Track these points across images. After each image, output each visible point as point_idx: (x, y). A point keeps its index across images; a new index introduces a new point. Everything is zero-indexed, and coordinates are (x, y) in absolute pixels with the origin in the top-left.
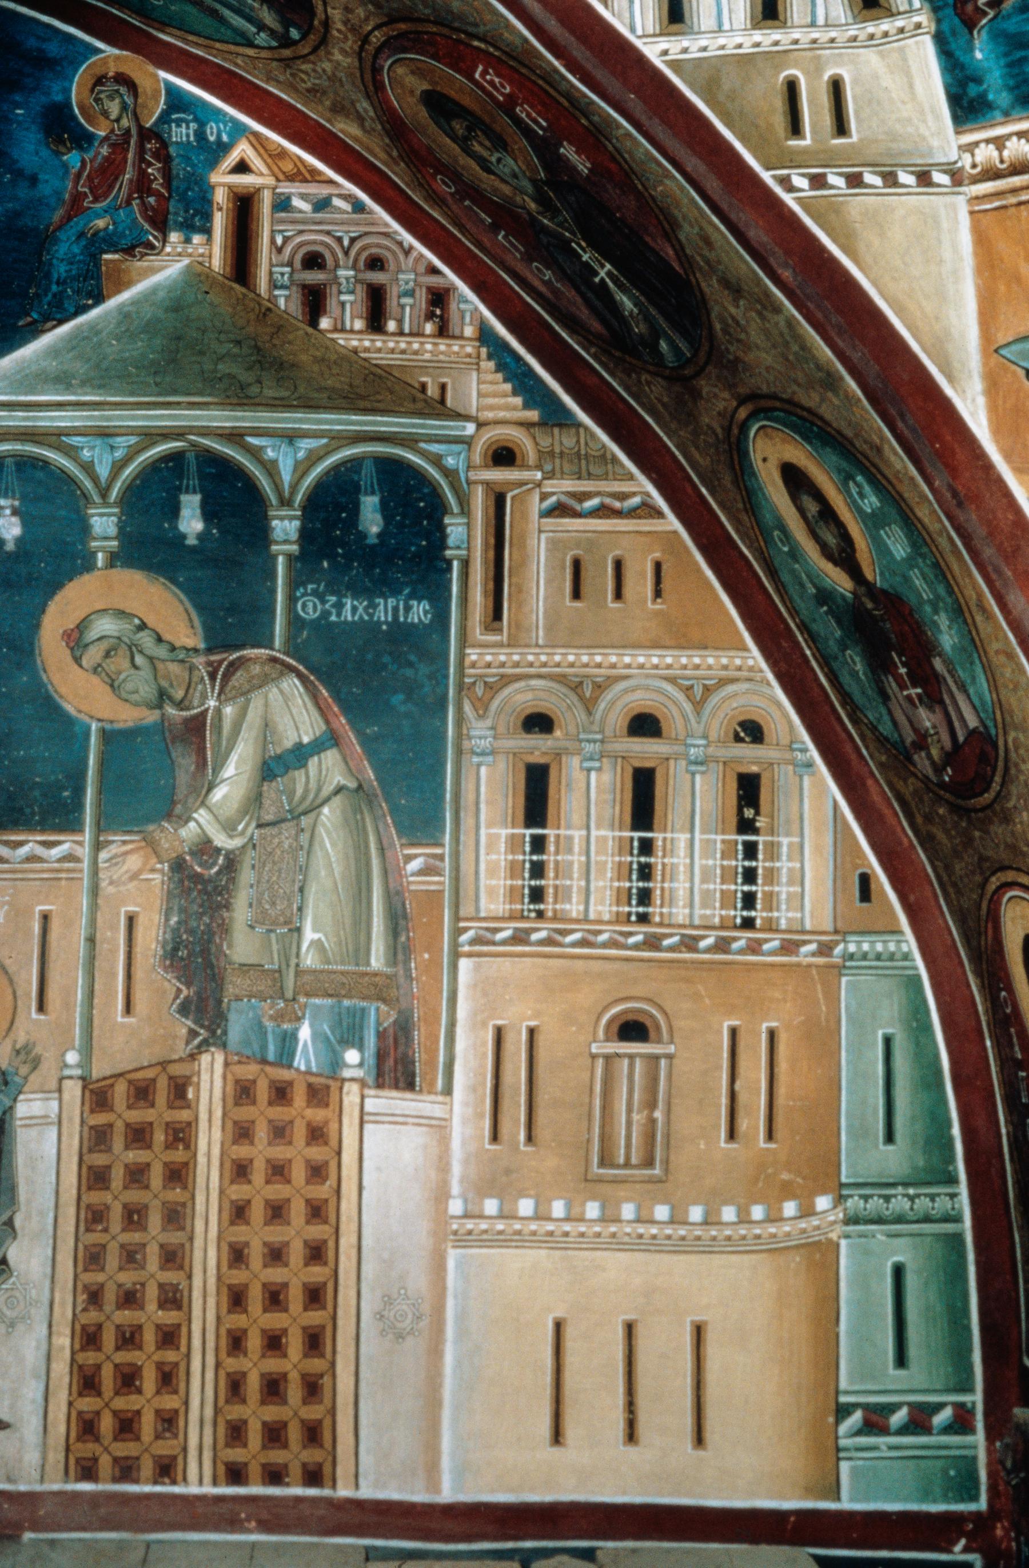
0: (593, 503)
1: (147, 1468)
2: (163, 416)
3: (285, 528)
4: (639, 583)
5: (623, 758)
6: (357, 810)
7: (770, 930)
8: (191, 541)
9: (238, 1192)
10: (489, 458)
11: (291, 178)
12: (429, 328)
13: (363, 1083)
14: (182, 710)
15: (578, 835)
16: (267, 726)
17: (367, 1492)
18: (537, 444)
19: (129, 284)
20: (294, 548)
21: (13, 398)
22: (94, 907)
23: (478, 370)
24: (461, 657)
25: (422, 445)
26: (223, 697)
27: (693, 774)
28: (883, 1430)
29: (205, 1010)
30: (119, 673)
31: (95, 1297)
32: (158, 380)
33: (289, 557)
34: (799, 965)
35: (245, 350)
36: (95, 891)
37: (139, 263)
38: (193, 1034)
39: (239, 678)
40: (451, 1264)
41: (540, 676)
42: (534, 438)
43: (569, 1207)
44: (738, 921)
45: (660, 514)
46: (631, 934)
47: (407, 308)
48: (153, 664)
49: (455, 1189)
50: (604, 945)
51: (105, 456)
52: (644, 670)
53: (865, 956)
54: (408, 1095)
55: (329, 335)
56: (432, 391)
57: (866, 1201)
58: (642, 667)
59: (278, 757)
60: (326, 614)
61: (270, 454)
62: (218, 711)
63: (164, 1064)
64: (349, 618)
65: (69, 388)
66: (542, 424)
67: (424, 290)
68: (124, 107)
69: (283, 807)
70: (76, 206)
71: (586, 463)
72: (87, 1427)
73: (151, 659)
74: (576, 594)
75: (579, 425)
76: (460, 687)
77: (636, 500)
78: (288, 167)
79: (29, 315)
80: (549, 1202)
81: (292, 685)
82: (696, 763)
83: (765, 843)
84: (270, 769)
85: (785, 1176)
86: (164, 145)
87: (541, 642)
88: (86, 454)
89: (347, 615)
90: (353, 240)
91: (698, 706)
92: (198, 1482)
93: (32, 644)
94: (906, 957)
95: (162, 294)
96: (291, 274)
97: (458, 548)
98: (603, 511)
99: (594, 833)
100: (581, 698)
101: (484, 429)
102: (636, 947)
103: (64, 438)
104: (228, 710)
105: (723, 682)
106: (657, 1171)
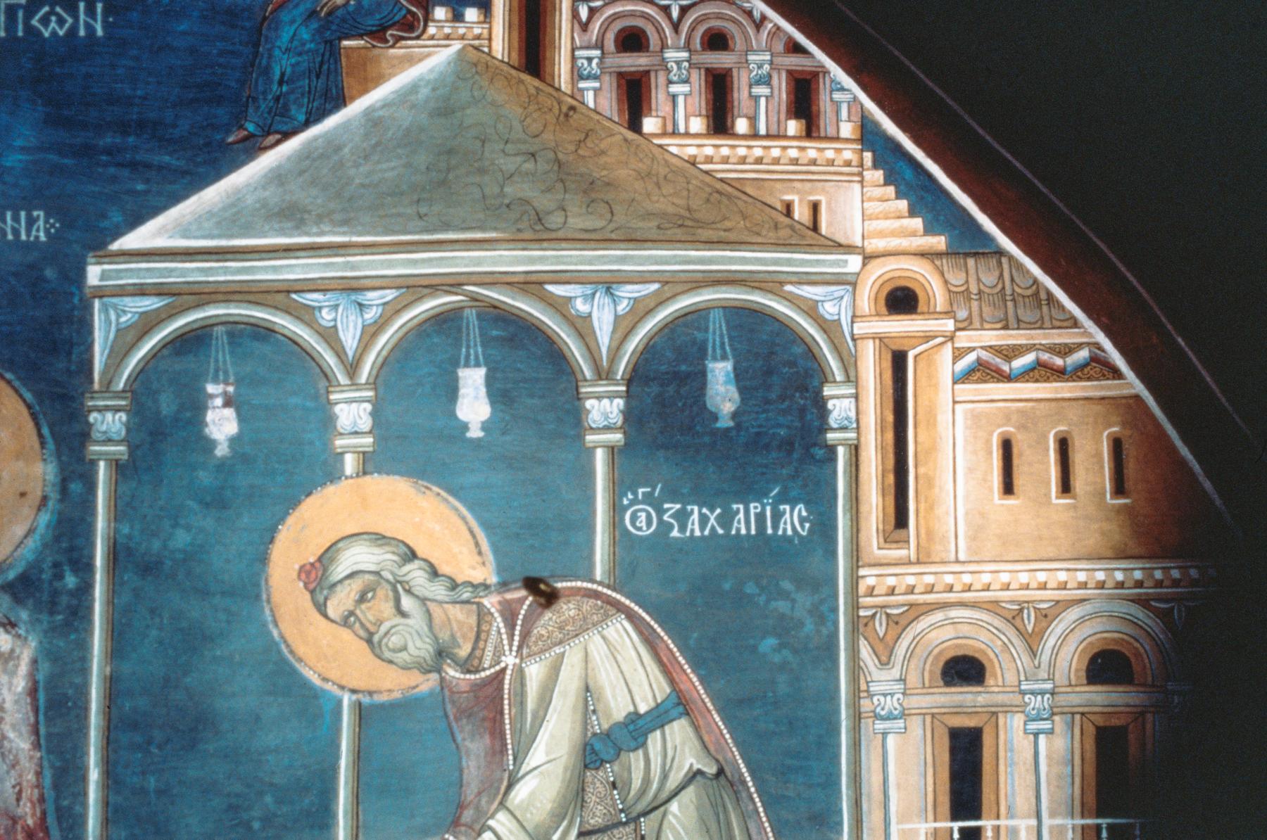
2: (430, 260)
3: (604, 409)
6: (718, 809)
10: (882, 302)
14: (469, 672)
18: (946, 282)
19: (379, 80)
20: (617, 437)
21: (224, 243)
23: (862, 182)
24: (854, 581)
25: (788, 288)
26: (525, 651)
30: (379, 623)
32: (423, 210)
33: (612, 449)
35: (542, 166)
37: (392, 51)
41: (962, 604)
42: (943, 275)
45: (1116, 374)
47: (761, 100)
48: (425, 605)
51: (352, 318)
55: (656, 141)
56: (801, 213)
59: (607, 735)
60: (665, 528)
61: (581, 306)
64: (697, 533)
65: (300, 226)
67: (784, 75)
69: (614, 805)
73: (423, 600)
74: (1008, 488)
75: (1000, 253)
76: (856, 625)
77: (1084, 354)
79: (242, 127)
81: (619, 631)
84: (593, 751)
88: (326, 316)
90: (684, 10)
93: (257, 585)
95: (424, 92)
96: (602, 58)
97: (843, 429)
99: (1047, 822)
100: (1021, 633)
101: (874, 263)
103: (294, 296)
104: (535, 672)
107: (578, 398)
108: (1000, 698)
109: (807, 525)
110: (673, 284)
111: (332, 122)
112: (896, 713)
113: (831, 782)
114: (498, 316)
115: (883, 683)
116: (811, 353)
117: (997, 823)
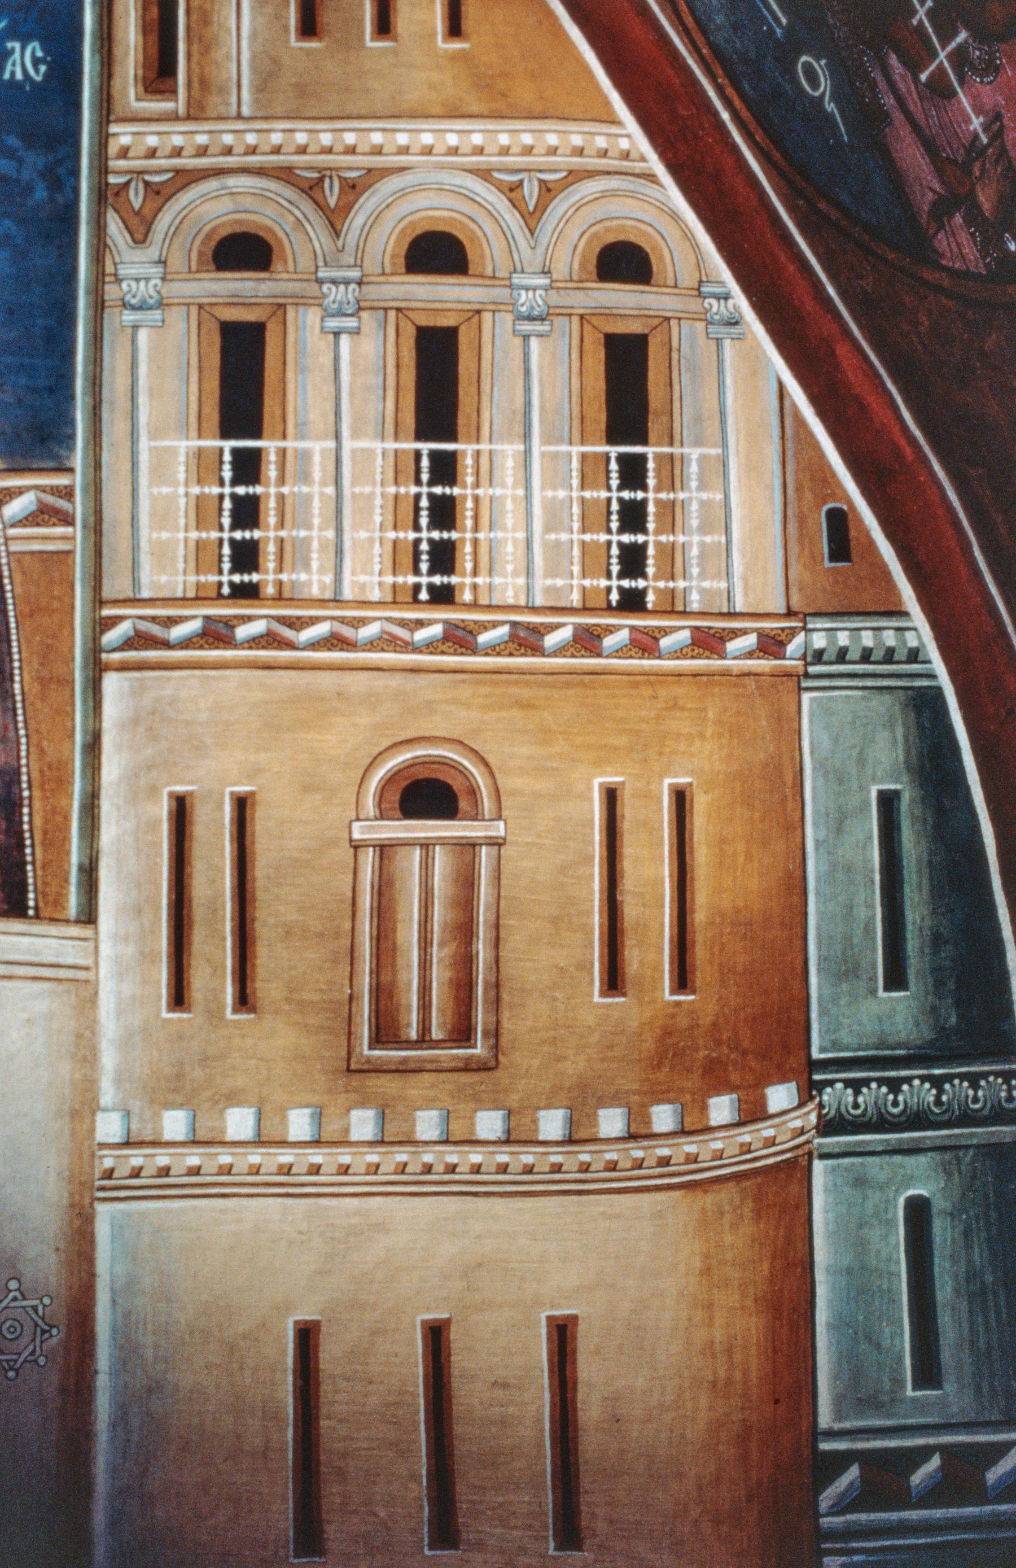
5: (399, 310)
7: (672, 612)
15: (319, 448)
27: (526, 337)
34: (726, 673)
40: (102, 1230)
43: (319, 1119)
44: (614, 597)
46: (420, 624)
49: (108, 1095)
50: (371, 645)
52: (435, 159)
54: (17, 925)
57: (857, 1093)
58: (428, 151)
76: (102, 194)
80: (282, 1112)
82: (531, 318)
83: (658, 457)
87: (246, 111)
91: (532, 219)
94: (914, 655)
99: (348, 444)
100: (321, 206)
102: (430, 647)
105: (575, 176)
106: (479, 1050)
108: (291, 287)
109: (43, 68)
112: (151, 302)
117: (281, 444)
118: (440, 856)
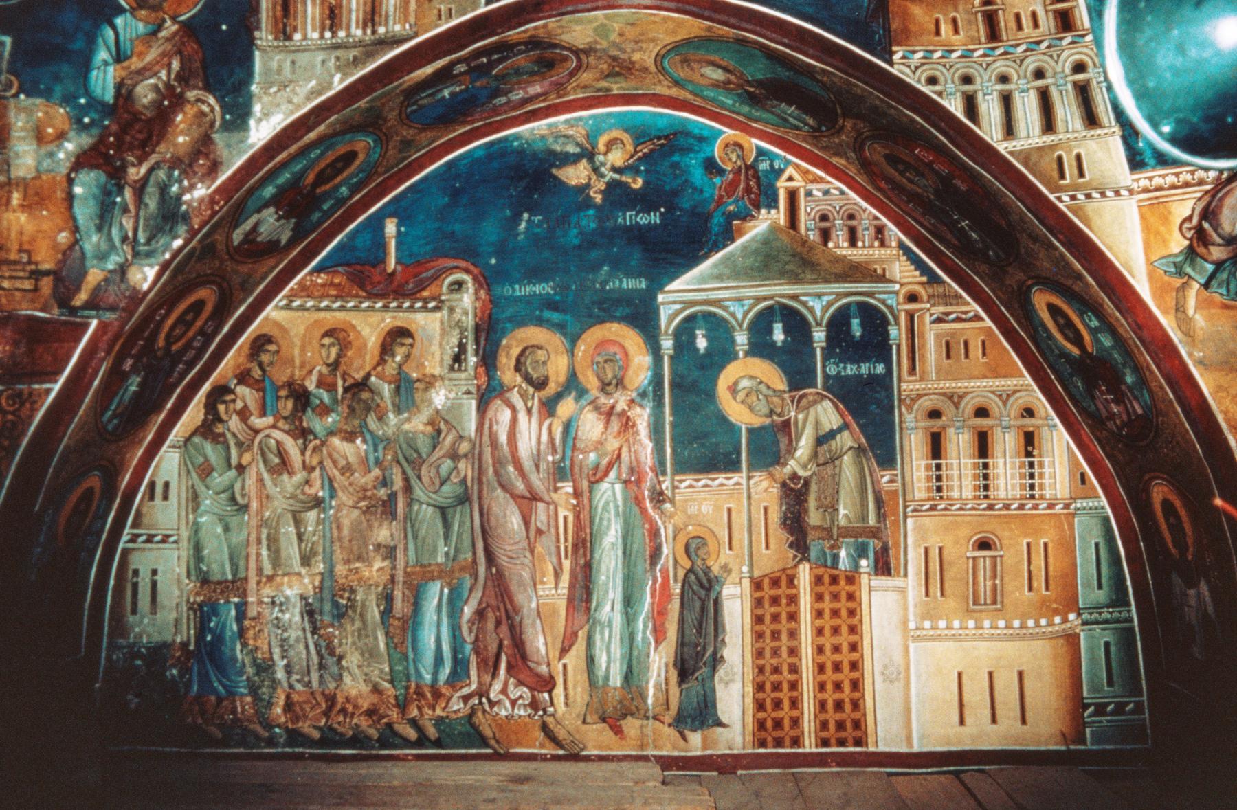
0: (954, 316)
1: (787, 741)
3: (819, 336)
4: (976, 350)
6: (858, 456)
8: (779, 344)
9: (818, 623)
11: (812, 182)
12: (876, 244)
13: (869, 574)
15: (955, 462)
16: (817, 423)
17: (882, 748)
19: (745, 233)
20: (824, 344)
22: (749, 504)
24: (899, 387)
28: (1104, 714)
29: (800, 546)
31: (761, 670)
33: (822, 348)
36: (749, 497)
38: (795, 556)
39: (804, 401)
40: (911, 650)
43: (961, 622)
45: (982, 319)
47: (866, 235)
49: (911, 617)
53: (1084, 509)
56: (879, 271)
60: (839, 372)
61: (811, 304)
62: (796, 417)
63: (784, 570)
65: (722, 281)
66: (929, 283)
68: (738, 156)
70: (720, 202)
71: (950, 298)
72: (761, 725)
73: (766, 396)
74: (948, 357)
75: (944, 282)
76: (900, 400)
77: (971, 314)
78: (811, 177)
81: (827, 404)
85: (1055, 606)
86: (756, 171)
88: (732, 309)
89: (849, 372)
91: (1005, 403)
92: (809, 746)
94: (1103, 508)
98: (958, 320)
102: (984, 509)
104: (801, 416)
105: (1015, 392)
107: (811, 332)
110: (839, 296)
111: (731, 248)
113: (894, 448)
114: (784, 307)
115: (909, 418)
116: (884, 316)
118: (988, 560)
